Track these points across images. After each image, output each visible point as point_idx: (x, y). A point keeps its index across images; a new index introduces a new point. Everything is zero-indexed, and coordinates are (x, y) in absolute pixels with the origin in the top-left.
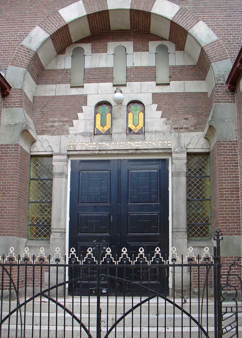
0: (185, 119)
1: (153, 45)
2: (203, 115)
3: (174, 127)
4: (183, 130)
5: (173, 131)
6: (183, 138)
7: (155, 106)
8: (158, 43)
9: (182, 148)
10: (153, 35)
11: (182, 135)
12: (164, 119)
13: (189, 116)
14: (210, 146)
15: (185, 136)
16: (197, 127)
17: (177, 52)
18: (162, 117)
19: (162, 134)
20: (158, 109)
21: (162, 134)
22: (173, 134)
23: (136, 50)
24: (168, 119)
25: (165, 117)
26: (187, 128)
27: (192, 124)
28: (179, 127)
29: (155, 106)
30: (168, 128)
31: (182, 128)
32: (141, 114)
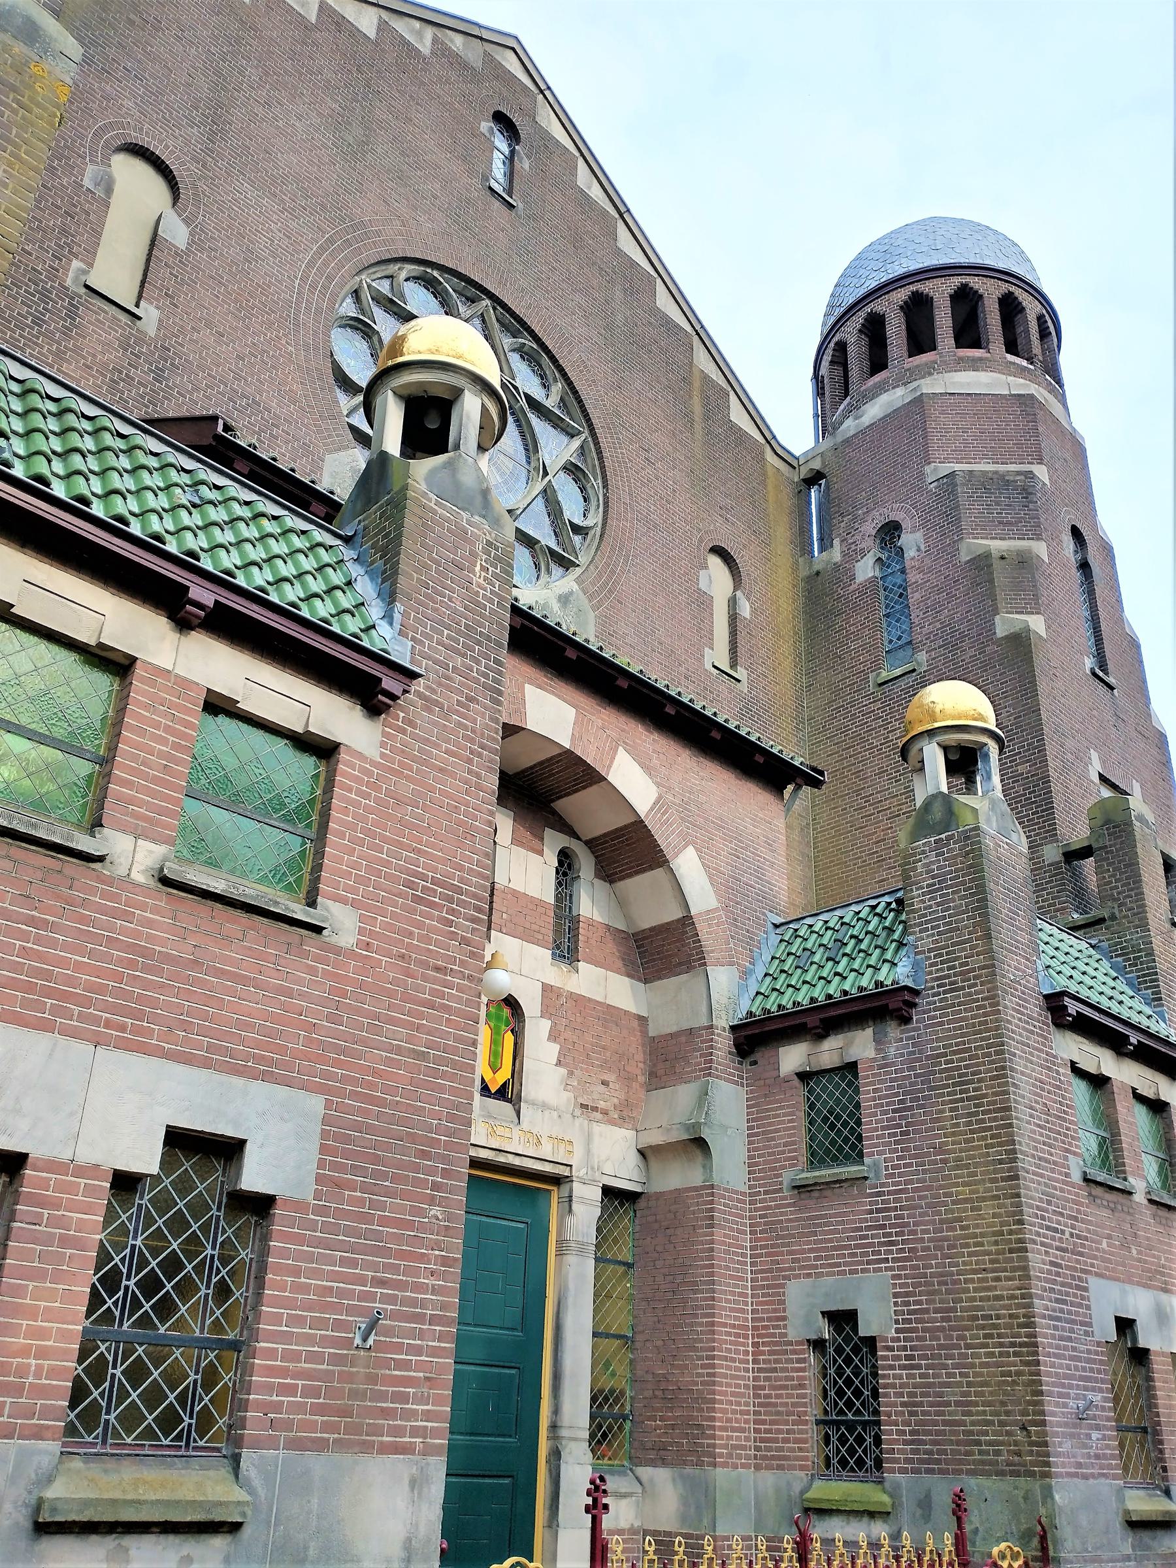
0: (605, 1083)
1: (554, 841)
2: (637, 1081)
3: (581, 1100)
4: (598, 1115)
5: (578, 1112)
6: (596, 1140)
7: (546, 1024)
8: (563, 841)
9: (593, 1168)
10: (554, 813)
11: (598, 1128)
12: (563, 1071)
13: (610, 1077)
14: (648, 1178)
15: (601, 1135)
16: (625, 1113)
17: (597, 882)
18: (559, 1063)
19: (555, 1114)
20: (553, 1036)
21: (555, 1114)
22: (577, 1122)
23: (516, 841)
24: (571, 1073)
25: (565, 1066)
26: (605, 1113)
27: (616, 1100)
28: (590, 1104)
29: (546, 1024)
30: (569, 1100)
31: (595, 1109)
32: (509, 1038)
